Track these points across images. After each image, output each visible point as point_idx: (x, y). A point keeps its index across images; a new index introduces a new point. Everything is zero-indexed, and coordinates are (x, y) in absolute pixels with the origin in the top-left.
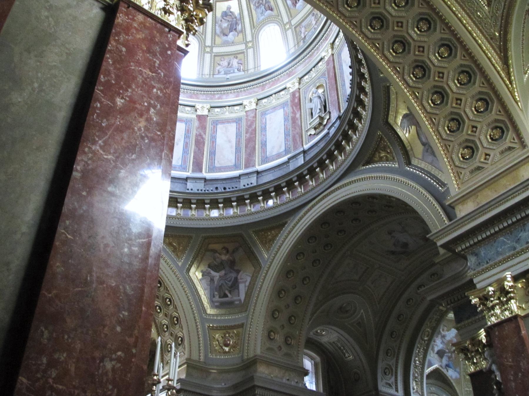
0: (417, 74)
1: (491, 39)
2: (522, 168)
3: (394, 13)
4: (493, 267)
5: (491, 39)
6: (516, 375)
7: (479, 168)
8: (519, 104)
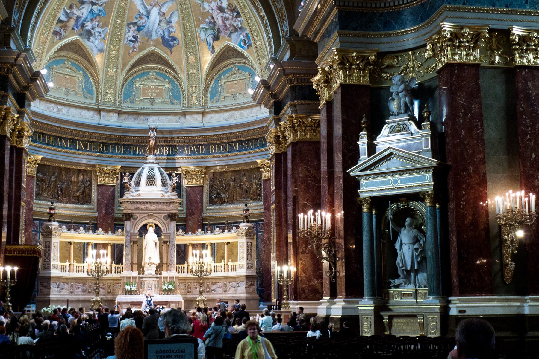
6: (465, 114)
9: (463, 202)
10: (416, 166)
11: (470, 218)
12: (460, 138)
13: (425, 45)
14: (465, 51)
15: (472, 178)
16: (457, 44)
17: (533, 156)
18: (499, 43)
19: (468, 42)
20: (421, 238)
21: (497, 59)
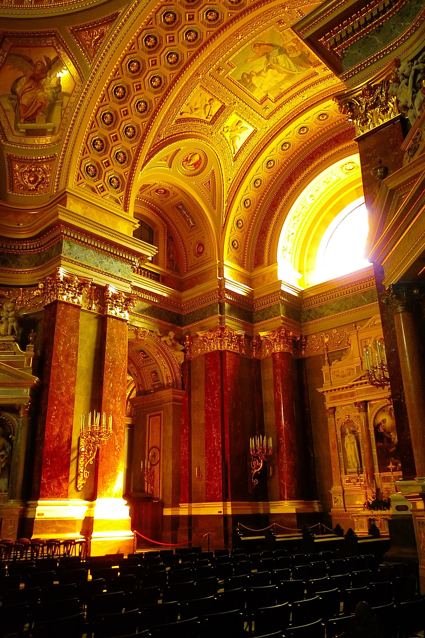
6: (65, 344)
9: (54, 415)
10: (15, 380)
11: (58, 430)
12: (59, 362)
13: (37, 285)
14: (72, 294)
15: (64, 396)
16: (67, 287)
17: (111, 385)
18: (97, 296)
19: (75, 287)
20: (7, 447)
21: (94, 307)
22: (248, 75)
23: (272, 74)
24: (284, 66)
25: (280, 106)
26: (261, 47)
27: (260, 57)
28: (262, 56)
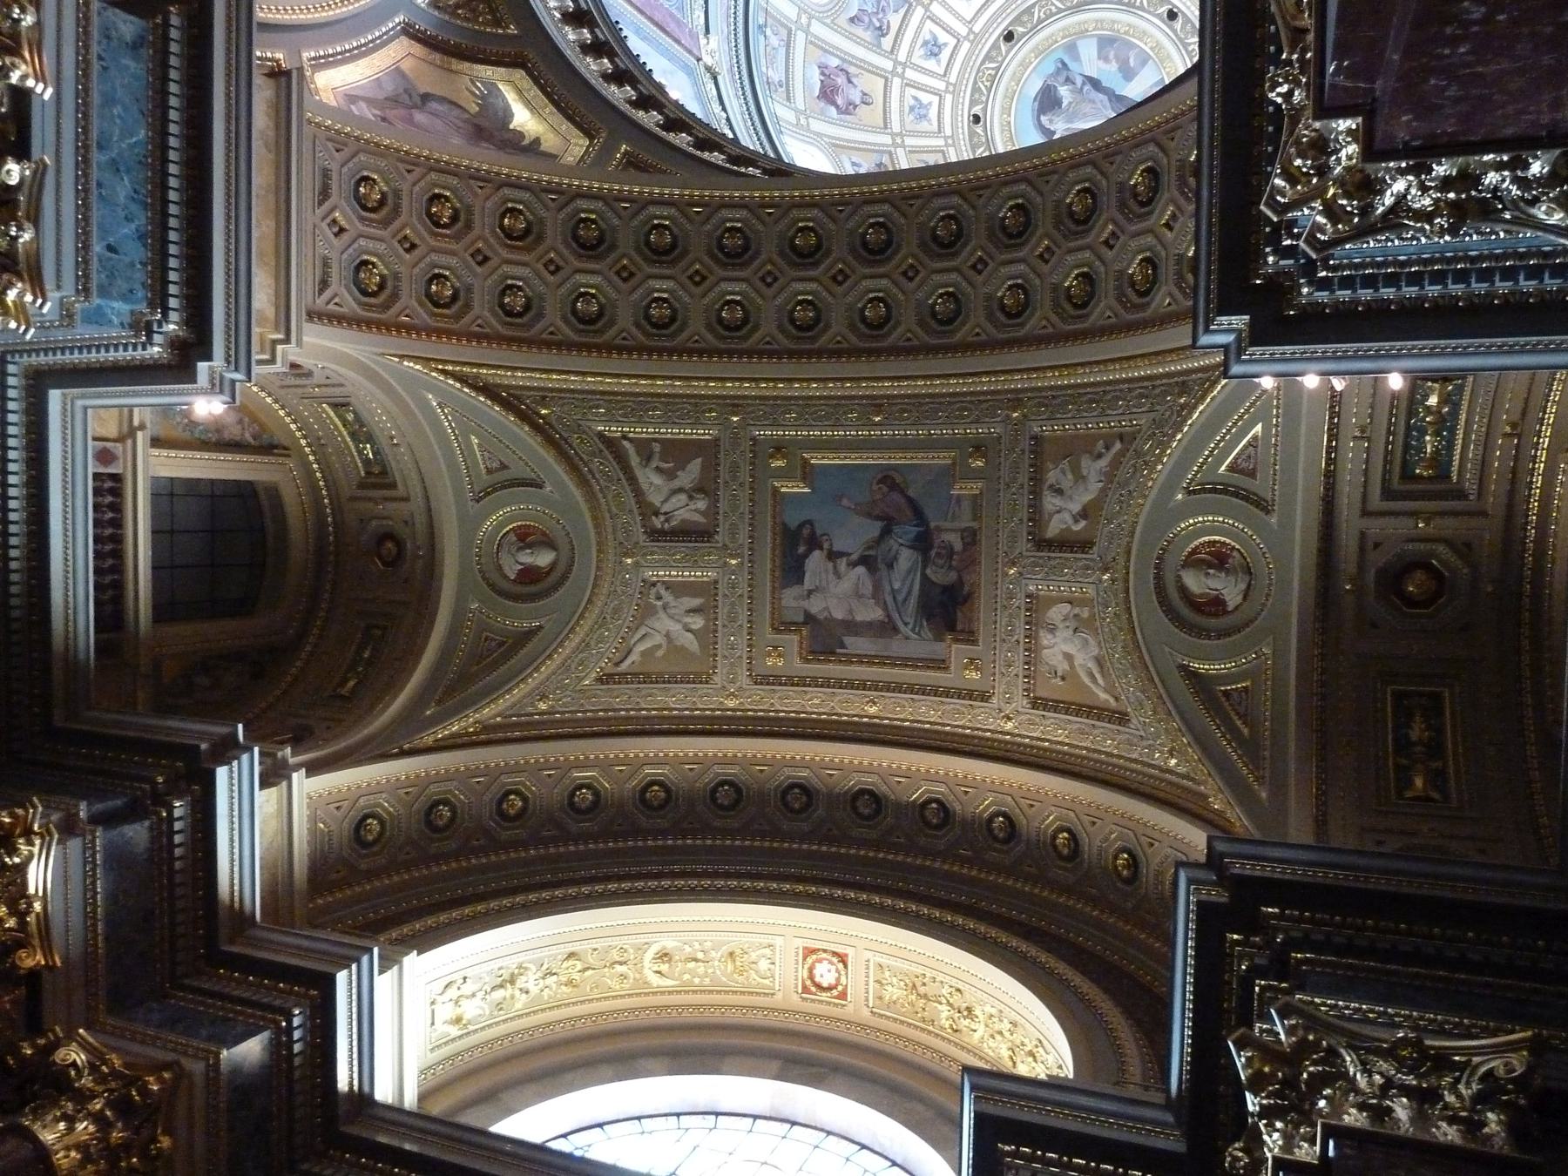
0: (589, 228)
1: (544, 398)
2: (271, 281)
3: (725, 286)
4: (84, 67)
5: (544, 397)
7: (325, 194)
8: (397, 360)
22: (813, 533)
23: (857, 585)
24: (897, 586)
25: (802, 682)
26: (896, 496)
27: (869, 515)
28: (878, 518)
